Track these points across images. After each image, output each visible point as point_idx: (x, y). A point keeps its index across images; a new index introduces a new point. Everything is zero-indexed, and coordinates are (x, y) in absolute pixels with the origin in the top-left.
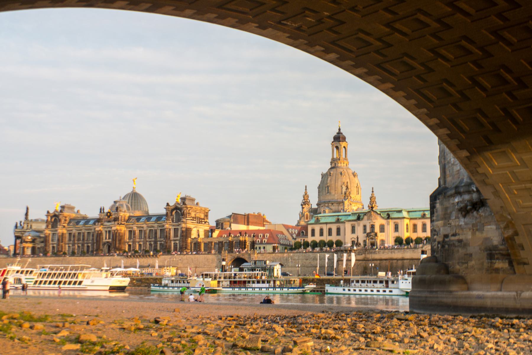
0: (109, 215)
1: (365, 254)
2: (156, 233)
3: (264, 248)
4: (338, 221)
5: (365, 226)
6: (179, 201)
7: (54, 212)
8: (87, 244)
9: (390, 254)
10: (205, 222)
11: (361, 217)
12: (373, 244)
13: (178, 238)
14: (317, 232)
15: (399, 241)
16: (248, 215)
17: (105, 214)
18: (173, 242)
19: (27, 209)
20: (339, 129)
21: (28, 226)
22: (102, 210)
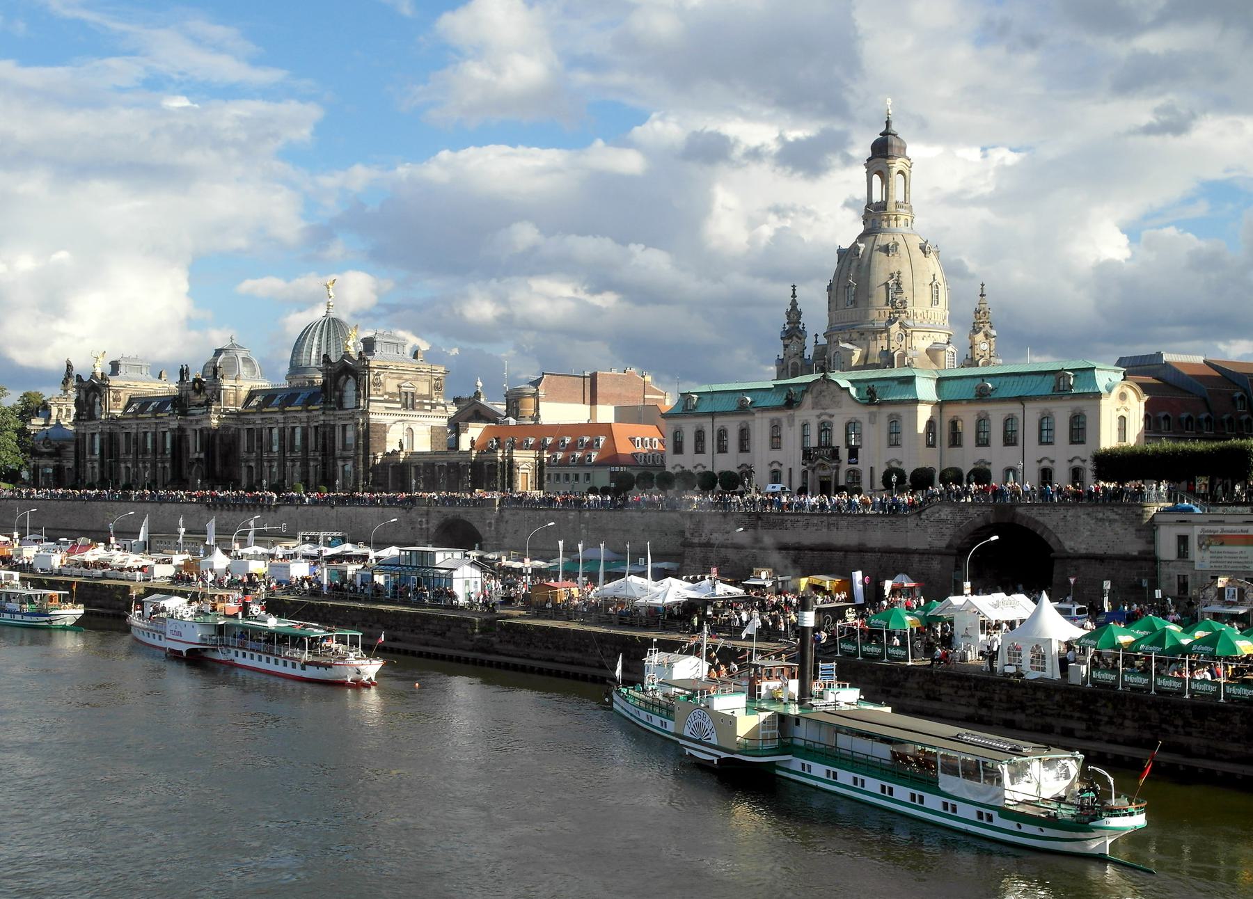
8: (163, 462)
9: (825, 530)
10: (433, 406)
21: (60, 410)
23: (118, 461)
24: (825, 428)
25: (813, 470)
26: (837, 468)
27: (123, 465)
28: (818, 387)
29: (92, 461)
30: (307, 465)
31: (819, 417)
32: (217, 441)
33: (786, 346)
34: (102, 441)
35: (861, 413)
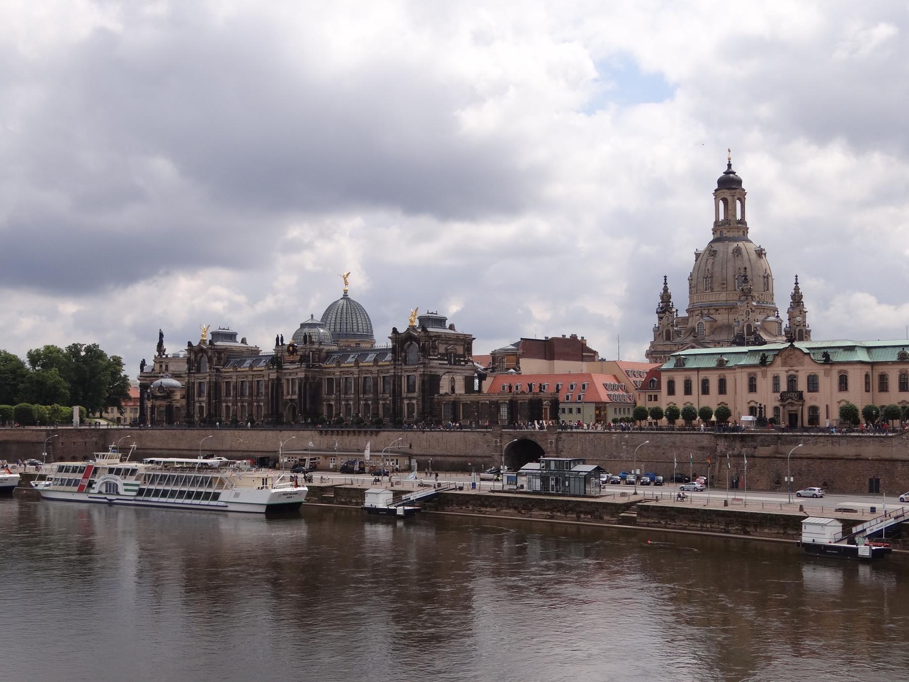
0: (292, 350)
1: (776, 444)
2: (376, 384)
3: (579, 410)
4: (721, 365)
5: (776, 379)
6: (417, 323)
7: (199, 345)
8: (258, 402)
9: (830, 446)
10: (466, 362)
11: (770, 359)
12: (793, 418)
13: (415, 395)
14: (679, 387)
15: (848, 414)
16: (553, 339)
17: (285, 348)
18: (406, 402)
19: (161, 335)
20: (729, 165)
21: (161, 366)
22: (279, 340)
23: (220, 402)
24: (792, 381)
25: (784, 406)
26: (803, 405)
27: (224, 404)
28: (786, 352)
29: (200, 402)
30: (378, 403)
31: (787, 372)
32: (308, 387)
33: (660, 318)
34: (210, 387)
35: (819, 371)
